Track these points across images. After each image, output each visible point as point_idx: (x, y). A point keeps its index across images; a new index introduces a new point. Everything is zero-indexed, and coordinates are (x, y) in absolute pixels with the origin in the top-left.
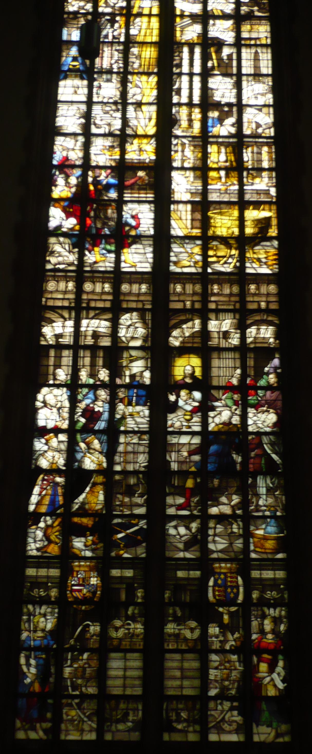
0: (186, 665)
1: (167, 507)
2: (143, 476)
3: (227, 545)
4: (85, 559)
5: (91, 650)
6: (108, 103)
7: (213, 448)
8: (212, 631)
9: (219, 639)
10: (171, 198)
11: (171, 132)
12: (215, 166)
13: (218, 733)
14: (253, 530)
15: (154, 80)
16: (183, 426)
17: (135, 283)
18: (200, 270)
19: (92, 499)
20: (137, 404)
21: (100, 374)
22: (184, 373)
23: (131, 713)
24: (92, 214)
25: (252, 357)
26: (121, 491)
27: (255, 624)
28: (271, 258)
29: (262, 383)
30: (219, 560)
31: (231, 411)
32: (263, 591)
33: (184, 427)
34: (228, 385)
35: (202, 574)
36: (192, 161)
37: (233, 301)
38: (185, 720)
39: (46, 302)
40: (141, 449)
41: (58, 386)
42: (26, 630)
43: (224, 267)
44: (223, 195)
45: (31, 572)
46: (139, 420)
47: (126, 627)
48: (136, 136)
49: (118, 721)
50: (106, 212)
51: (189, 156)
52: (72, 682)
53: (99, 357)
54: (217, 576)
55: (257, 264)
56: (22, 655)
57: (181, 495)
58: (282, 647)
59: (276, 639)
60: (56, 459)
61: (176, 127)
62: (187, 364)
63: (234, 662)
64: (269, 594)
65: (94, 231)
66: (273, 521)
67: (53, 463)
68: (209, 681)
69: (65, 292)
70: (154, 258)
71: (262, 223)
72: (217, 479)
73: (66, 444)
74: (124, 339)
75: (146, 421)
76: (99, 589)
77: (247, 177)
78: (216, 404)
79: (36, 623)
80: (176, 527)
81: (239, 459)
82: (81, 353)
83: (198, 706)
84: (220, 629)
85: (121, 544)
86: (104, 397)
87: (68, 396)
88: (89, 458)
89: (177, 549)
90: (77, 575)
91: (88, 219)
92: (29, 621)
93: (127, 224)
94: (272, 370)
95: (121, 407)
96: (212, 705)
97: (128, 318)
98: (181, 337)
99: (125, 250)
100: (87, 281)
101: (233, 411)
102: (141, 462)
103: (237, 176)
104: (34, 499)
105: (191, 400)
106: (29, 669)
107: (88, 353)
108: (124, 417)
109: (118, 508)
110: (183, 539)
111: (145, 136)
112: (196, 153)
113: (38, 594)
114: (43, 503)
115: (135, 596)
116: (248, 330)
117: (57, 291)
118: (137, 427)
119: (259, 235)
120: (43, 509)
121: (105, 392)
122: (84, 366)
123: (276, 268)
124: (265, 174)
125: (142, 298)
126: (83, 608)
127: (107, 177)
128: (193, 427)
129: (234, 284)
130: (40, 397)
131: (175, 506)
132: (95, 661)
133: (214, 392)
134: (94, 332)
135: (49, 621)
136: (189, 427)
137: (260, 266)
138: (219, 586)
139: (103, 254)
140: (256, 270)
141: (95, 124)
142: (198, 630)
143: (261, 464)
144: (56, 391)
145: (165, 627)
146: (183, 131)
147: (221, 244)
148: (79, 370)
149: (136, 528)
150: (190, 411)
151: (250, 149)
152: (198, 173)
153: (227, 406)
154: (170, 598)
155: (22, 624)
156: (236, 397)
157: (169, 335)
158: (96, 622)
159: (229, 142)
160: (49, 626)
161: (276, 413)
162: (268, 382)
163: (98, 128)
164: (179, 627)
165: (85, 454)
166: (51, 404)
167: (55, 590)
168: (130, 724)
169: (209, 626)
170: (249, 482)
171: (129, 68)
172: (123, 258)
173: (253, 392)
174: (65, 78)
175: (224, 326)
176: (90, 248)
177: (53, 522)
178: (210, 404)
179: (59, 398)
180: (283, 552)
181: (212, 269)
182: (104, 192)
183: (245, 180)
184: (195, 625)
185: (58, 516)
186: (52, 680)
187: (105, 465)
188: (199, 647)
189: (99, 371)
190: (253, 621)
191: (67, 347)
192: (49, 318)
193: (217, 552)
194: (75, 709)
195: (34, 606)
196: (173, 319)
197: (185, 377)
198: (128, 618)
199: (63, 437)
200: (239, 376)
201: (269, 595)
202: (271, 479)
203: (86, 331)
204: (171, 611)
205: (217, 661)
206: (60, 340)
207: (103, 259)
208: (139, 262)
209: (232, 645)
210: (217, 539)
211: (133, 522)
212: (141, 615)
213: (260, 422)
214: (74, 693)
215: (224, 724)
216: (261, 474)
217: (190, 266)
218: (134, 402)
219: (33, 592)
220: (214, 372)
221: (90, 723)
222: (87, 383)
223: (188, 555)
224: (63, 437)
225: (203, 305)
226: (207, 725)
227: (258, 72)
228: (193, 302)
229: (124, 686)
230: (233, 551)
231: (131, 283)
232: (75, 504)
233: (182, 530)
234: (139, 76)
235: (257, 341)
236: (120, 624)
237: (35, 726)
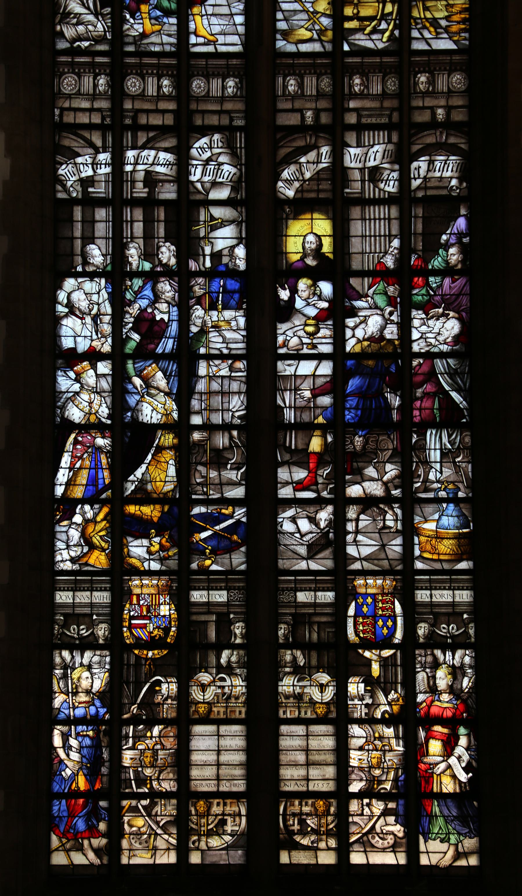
0: (314, 743)
1: (279, 485)
2: (238, 434)
3: (377, 548)
4: (150, 573)
5: (166, 722)
7: (353, 383)
8: (353, 689)
9: (364, 702)
13: (365, 852)
14: (419, 523)
16: (303, 344)
17: (215, 75)
18: (329, 47)
19: (156, 474)
20: (226, 307)
21: (162, 253)
22: (304, 248)
23: (229, 820)
25: (421, 215)
26: (204, 460)
27: (421, 677)
28: (456, 18)
29: (437, 263)
30: (364, 573)
31: (383, 315)
32: (434, 624)
33: (305, 346)
34: (378, 268)
35: (336, 597)
37: (387, 109)
38: (315, 831)
39: (61, 116)
40: (235, 386)
41: (92, 276)
42: (62, 692)
43: (372, 40)
45: (64, 598)
46: (229, 335)
47: (218, 684)
49: (210, 834)
52: (136, 772)
53: (158, 221)
54: (360, 600)
55: (430, 32)
56: (56, 732)
57: (302, 464)
58: (465, 715)
59: (455, 702)
60: (95, 406)
62: (310, 231)
63: (389, 738)
64: (444, 628)
66: (452, 506)
67: (90, 414)
68: (350, 769)
69: (94, 96)
70: (247, 24)
72: (360, 437)
73: (110, 379)
74: (199, 186)
75: (242, 338)
76: (173, 623)
78: (359, 304)
79: (75, 681)
80: (293, 520)
81: (396, 402)
82: (127, 213)
83: (332, 809)
84: (365, 686)
85: (208, 549)
86: (170, 294)
87: (108, 293)
88: (149, 403)
89: (297, 557)
90: (138, 600)
92: (65, 676)
94: (453, 240)
95: (199, 312)
96: (354, 806)
97: (205, 146)
98: (298, 180)
99: (196, 10)
100: (132, 73)
101: (387, 316)
102: (234, 410)
104: (62, 476)
105: (316, 298)
106: (68, 755)
107: (139, 214)
108: (203, 331)
109: (199, 488)
110: (307, 538)
113: (78, 634)
114: (77, 483)
115: (231, 633)
116: (415, 164)
117: (79, 93)
118: (227, 348)
120: (78, 492)
121: (170, 284)
122: (133, 238)
123: (465, 39)
125: (228, 106)
126: (150, 654)
128: (319, 346)
129: (390, 73)
130: (62, 296)
131: (292, 483)
132: (171, 739)
133: (354, 282)
134: (148, 173)
135: (96, 676)
136: (314, 346)
137: (437, 37)
138: (365, 616)
139: (156, 18)
140: (429, 45)
142: (331, 688)
143: (433, 409)
144: (89, 286)
145: (280, 683)
148: (125, 246)
149: (230, 522)
150: (314, 318)
153: (377, 307)
154: (286, 636)
155: (55, 681)
156: (391, 289)
157: (277, 177)
158: (172, 676)
160: (97, 685)
161: (460, 319)
162: (447, 262)
164: (301, 684)
165: (143, 397)
166: (82, 308)
167: (103, 626)
168: (228, 838)
169: (350, 681)
170: (414, 441)
172: (192, 25)
173: (420, 280)
175: (372, 159)
176: (133, 5)
177: (96, 515)
178: (347, 304)
179: (95, 298)
180: (467, 560)
181: (349, 44)
184: (326, 680)
185: (103, 503)
186: (104, 770)
187: (175, 415)
188: (333, 715)
189: (159, 248)
190: (419, 672)
191: (102, 202)
192: (69, 148)
193: (360, 559)
194: (143, 816)
195: (71, 653)
196: (282, 147)
197: (305, 255)
198: (220, 668)
199: (104, 367)
200: (396, 251)
201: (443, 630)
202: (449, 436)
203: (134, 171)
204: (288, 658)
205: (363, 737)
206: (91, 190)
207: (157, 27)
208: (220, 34)
209: (385, 712)
210: (360, 537)
211: (223, 511)
212: (241, 664)
213: (433, 336)
214: (140, 790)
215: (373, 838)
216: (432, 427)
217: (311, 40)
218: (220, 302)
219: (70, 632)
220: (356, 245)
221: (166, 837)
222: (140, 269)
223: (314, 566)
224: (104, 367)
225: (334, 118)
226: (348, 839)
228: (317, 112)
229: (218, 779)
230: (388, 559)
231: (208, 76)
232: (129, 484)
233: (304, 525)
235: (428, 185)
236: (209, 680)
237: (82, 845)
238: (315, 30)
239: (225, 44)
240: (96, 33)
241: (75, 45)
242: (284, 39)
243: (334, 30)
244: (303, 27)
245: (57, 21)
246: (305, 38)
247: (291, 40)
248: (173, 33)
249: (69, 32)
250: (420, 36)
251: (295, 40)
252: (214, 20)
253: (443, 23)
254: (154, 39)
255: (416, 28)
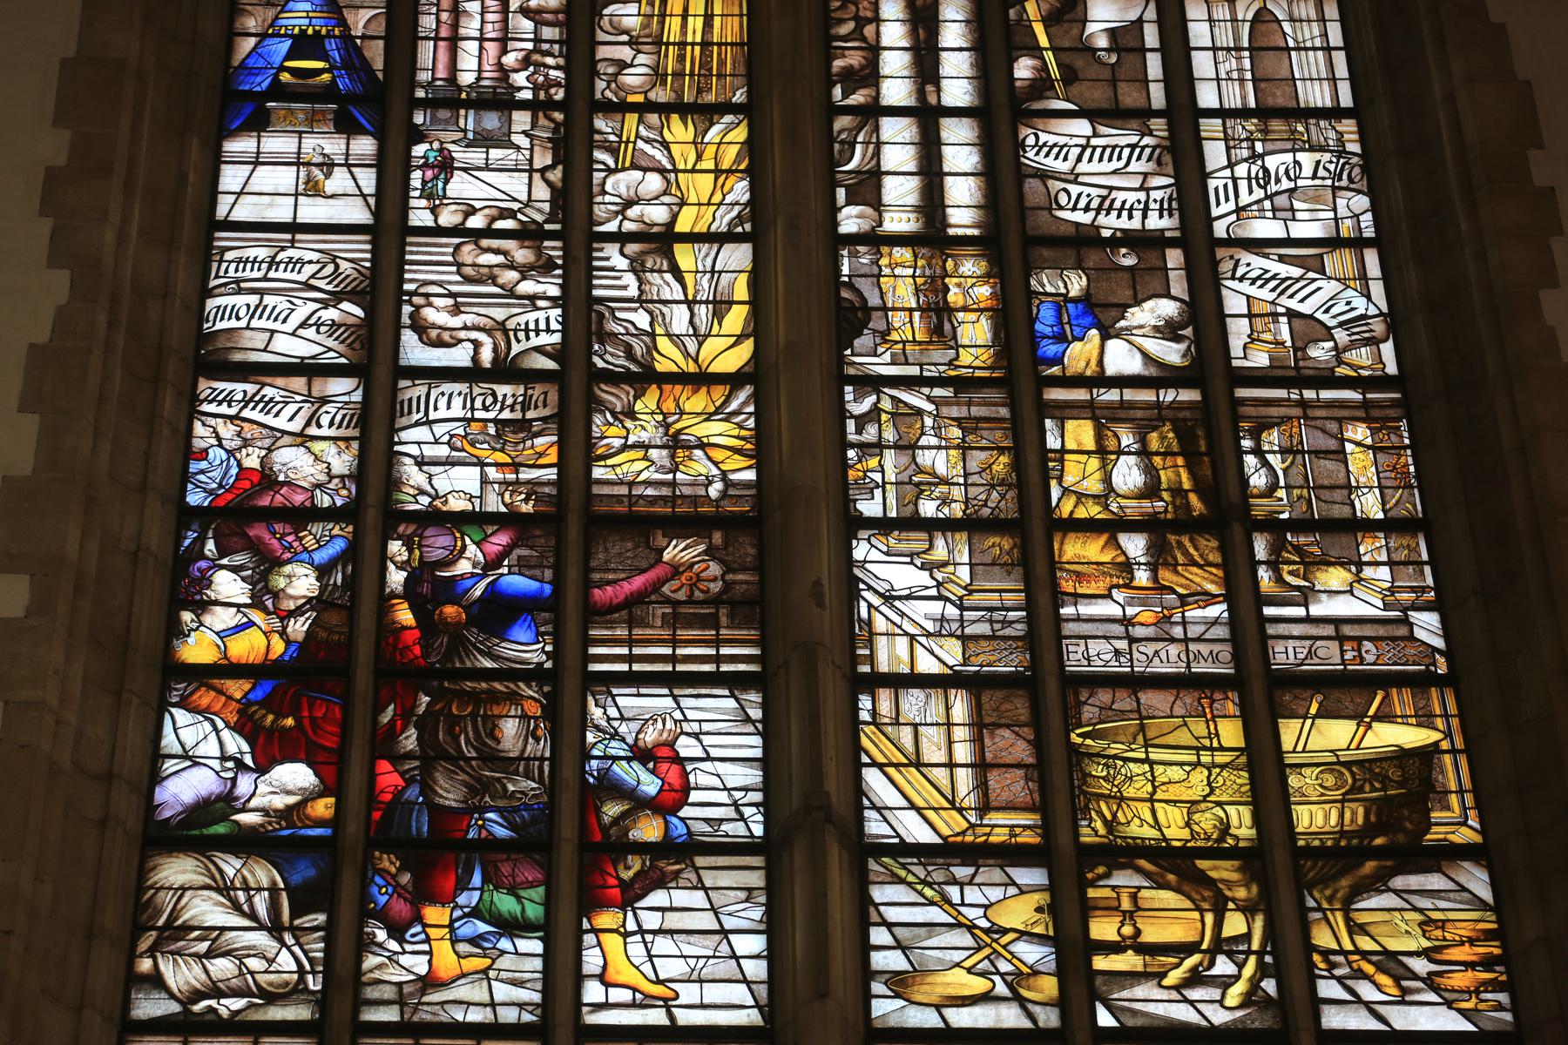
6: (489, 232)
10: (855, 660)
11: (841, 361)
12: (1092, 511)
15: (730, 137)
24: (410, 740)
36: (957, 492)
43: (1192, 1003)
44: (1150, 649)
48: (645, 377)
50: (493, 732)
51: (941, 469)
55: (1379, 987)
61: (864, 341)
65: (421, 824)
70: (772, 956)
71: (1385, 781)
77: (1274, 565)
91: (384, 766)
93: (612, 788)
99: (606, 919)
103: (1215, 557)
111: (701, 379)
112: (977, 459)
119: (1379, 841)
123: (1499, 1007)
124: (1371, 547)
127: (491, 564)
139: (474, 941)
140: (1382, 1019)
141: (420, 327)
146: (901, 359)
147: (1162, 885)
151: (1272, 439)
152: (997, 545)
159: (1158, 405)
163: (439, 343)
171: (600, 85)
172: (592, 961)
174: (259, 123)
176: (401, 908)
182: (472, 635)
183: (1264, 574)
217: (986, 998)
227: (1280, 99)
234: (653, 118)
238: (998, 972)
239: (703, 1006)
240: (272, 977)
241: (199, 1007)
242: (897, 996)
243: (1061, 973)
244: (958, 965)
245: (144, 945)
246: (966, 993)
247: (919, 998)
248: (527, 976)
249: (181, 974)
250: (1348, 997)
251: (934, 999)
252: (662, 945)
253: (1421, 966)
254: (462, 991)
255: (1333, 977)
